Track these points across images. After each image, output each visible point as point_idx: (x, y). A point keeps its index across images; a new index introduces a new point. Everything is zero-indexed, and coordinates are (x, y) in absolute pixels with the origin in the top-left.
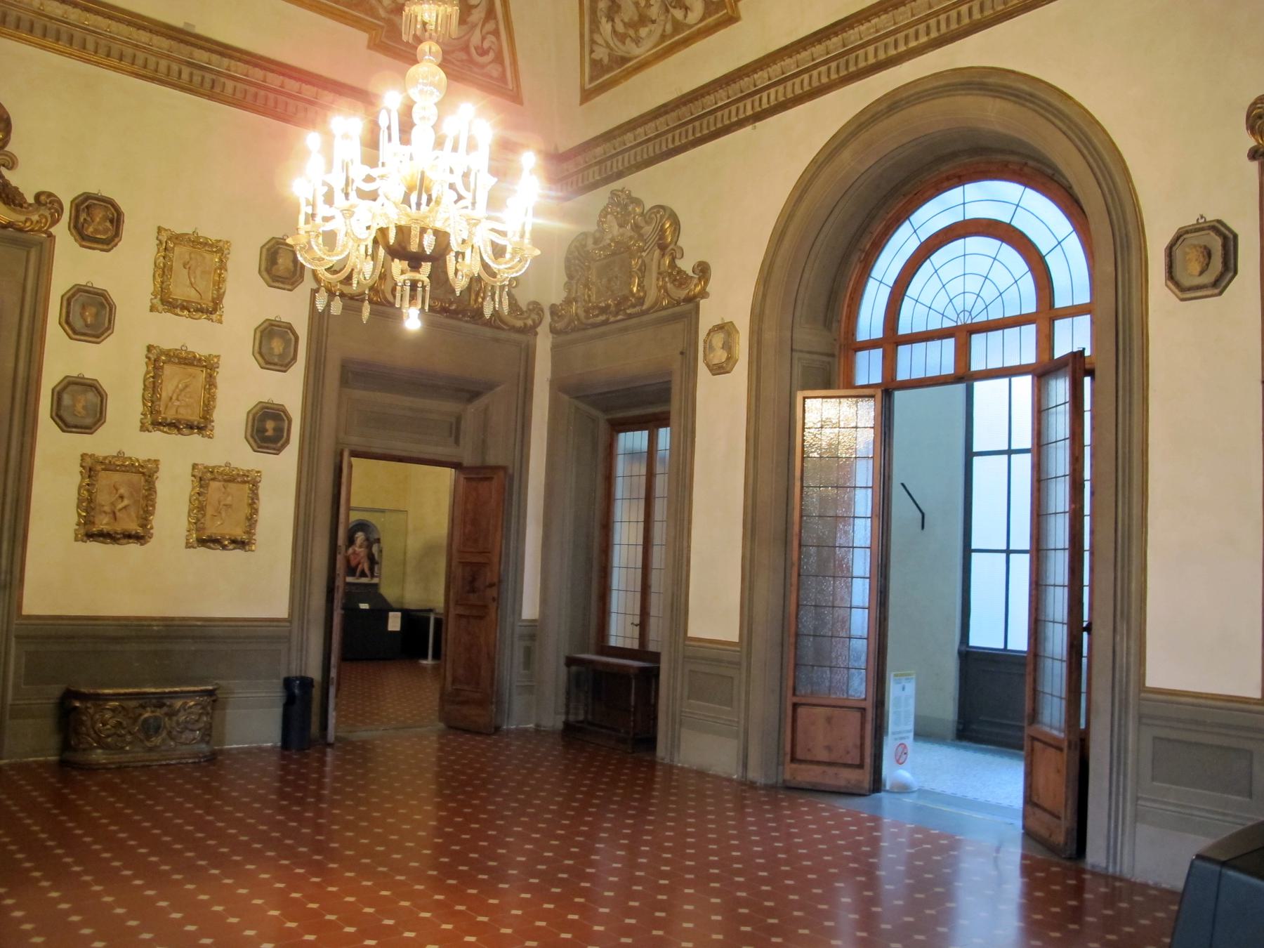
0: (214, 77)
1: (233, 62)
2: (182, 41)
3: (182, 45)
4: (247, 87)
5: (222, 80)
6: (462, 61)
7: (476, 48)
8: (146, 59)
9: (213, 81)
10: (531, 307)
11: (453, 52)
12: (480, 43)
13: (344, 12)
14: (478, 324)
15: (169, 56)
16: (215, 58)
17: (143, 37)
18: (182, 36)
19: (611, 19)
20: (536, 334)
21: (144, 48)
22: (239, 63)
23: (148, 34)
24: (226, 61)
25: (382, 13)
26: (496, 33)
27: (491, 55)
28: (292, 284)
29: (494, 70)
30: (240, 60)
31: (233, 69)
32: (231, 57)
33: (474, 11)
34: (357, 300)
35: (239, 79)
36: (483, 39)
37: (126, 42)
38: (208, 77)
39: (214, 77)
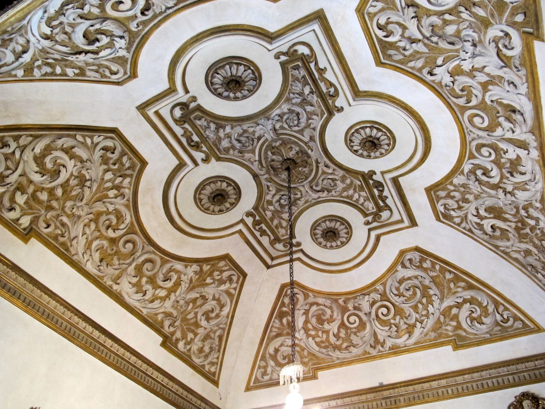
0: (395, 399)
1: (399, 389)
2: (376, 392)
3: (378, 393)
4: (409, 396)
5: (399, 398)
6: (500, 330)
7: (502, 321)
8: (368, 405)
9: (395, 400)
11: (493, 329)
12: (502, 318)
13: (435, 343)
15: (375, 400)
16: (391, 391)
17: (364, 397)
18: (376, 390)
19: (537, 272)
21: (366, 401)
22: (402, 388)
23: (365, 395)
24: (396, 390)
25: (451, 334)
26: (506, 309)
27: (511, 320)
29: (518, 324)
30: (401, 387)
31: (400, 392)
32: (397, 388)
33: (489, 307)
35: (405, 394)
36: (502, 316)
37: (359, 402)
38: (393, 400)
39: (395, 399)
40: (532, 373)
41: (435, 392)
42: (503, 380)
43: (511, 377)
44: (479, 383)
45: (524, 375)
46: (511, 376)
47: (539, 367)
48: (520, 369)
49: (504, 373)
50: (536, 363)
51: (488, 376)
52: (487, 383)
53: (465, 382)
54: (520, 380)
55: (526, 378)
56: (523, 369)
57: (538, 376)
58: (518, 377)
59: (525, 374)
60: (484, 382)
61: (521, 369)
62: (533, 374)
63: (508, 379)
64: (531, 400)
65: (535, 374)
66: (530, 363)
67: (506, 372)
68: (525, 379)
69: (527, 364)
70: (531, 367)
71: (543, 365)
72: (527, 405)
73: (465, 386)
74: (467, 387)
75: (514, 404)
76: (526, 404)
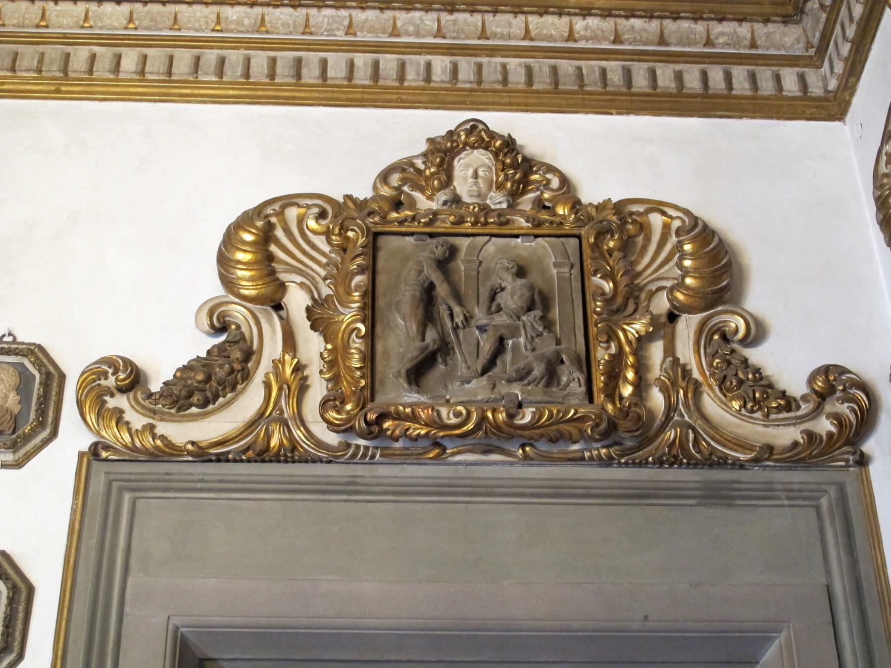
10: (819, 384)
14: (642, 464)
20: (863, 461)
28: (14, 446)
34: (220, 459)
40: (542, 66)
41: (53, 52)
42: (402, 66)
43: (441, 64)
44: (285, 57)
45: (504, 66)
46: (447, 59)
47: (581, 45)
48: (495, 36)
49: (417, 34)
50: (580, 24)
51: (340, 36)
52: (324, 63)
53: (223, 40)
54: (480, 82)
55: (511, 78)
56: (509, 37)
57: (568, 84)
58: (473, 68)
59: (514, 64)
60: (312, 58)
61: (502, 37)
62: (546, 70)
63: (429, 65)
64: (496, 155)
65: (554, 70)
66: (549, 19)
67: (429, 34)
68: (505, 81)
69: (533, 20)
70: (549, 38)
71: (605, 39)
72: (470, 172)
73: (211, 56)
74: (222, 61)
75: (412, 165)
76: (467, 166)
